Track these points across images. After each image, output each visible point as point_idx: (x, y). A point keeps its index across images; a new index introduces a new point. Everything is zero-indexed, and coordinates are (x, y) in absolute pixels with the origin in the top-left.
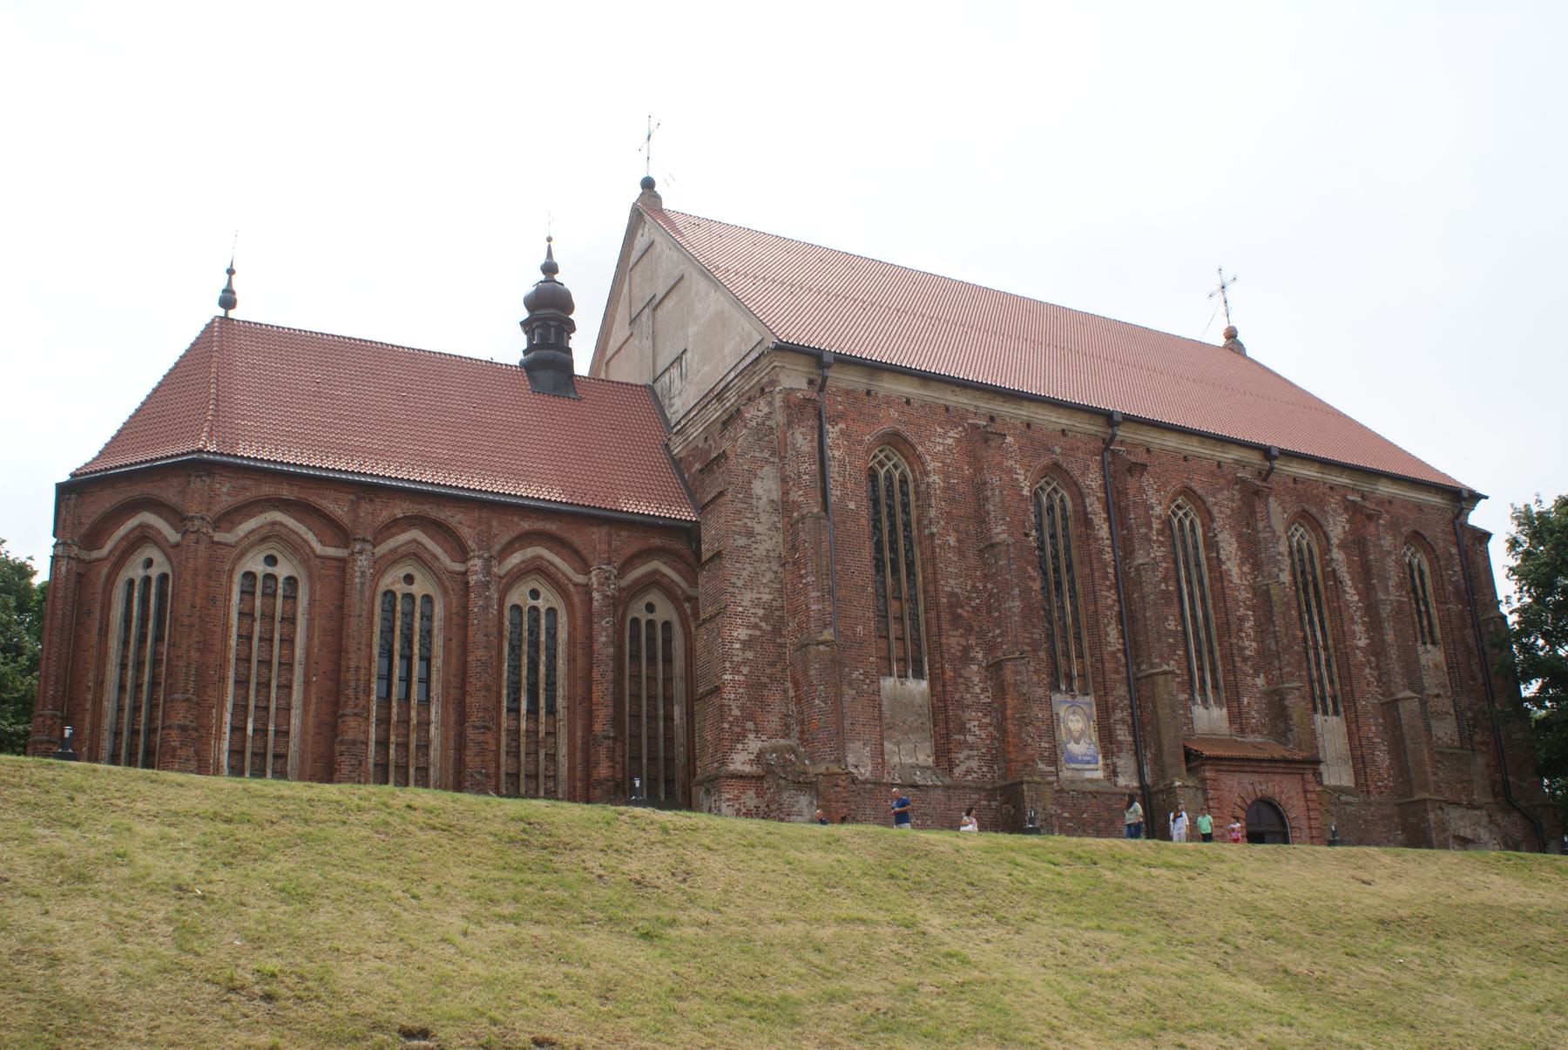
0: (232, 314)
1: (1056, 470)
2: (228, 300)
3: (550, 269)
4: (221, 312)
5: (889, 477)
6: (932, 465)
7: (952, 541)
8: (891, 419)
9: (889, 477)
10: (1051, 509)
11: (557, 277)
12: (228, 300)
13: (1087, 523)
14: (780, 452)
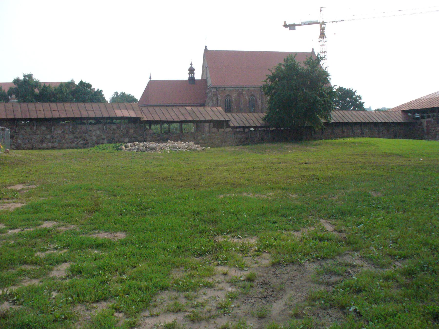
0: (151, 80)
1: (252, 95)
2: (150, 78)
3: (191, 64)
4: (150, 80)
5: (228, 99)
6: (233, 98)
7: (236, 107)
8: (228, 93)
9: (228, 99)
10: (252, 100)
11: (193, 66)
12: (150, 78)
13: (257, 102)
14: (212, 100)
